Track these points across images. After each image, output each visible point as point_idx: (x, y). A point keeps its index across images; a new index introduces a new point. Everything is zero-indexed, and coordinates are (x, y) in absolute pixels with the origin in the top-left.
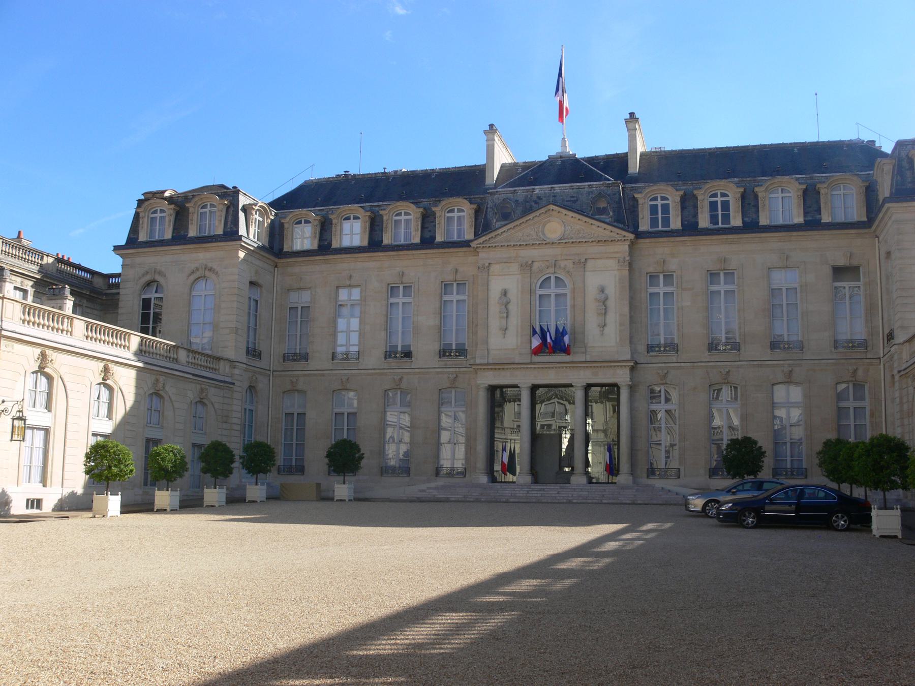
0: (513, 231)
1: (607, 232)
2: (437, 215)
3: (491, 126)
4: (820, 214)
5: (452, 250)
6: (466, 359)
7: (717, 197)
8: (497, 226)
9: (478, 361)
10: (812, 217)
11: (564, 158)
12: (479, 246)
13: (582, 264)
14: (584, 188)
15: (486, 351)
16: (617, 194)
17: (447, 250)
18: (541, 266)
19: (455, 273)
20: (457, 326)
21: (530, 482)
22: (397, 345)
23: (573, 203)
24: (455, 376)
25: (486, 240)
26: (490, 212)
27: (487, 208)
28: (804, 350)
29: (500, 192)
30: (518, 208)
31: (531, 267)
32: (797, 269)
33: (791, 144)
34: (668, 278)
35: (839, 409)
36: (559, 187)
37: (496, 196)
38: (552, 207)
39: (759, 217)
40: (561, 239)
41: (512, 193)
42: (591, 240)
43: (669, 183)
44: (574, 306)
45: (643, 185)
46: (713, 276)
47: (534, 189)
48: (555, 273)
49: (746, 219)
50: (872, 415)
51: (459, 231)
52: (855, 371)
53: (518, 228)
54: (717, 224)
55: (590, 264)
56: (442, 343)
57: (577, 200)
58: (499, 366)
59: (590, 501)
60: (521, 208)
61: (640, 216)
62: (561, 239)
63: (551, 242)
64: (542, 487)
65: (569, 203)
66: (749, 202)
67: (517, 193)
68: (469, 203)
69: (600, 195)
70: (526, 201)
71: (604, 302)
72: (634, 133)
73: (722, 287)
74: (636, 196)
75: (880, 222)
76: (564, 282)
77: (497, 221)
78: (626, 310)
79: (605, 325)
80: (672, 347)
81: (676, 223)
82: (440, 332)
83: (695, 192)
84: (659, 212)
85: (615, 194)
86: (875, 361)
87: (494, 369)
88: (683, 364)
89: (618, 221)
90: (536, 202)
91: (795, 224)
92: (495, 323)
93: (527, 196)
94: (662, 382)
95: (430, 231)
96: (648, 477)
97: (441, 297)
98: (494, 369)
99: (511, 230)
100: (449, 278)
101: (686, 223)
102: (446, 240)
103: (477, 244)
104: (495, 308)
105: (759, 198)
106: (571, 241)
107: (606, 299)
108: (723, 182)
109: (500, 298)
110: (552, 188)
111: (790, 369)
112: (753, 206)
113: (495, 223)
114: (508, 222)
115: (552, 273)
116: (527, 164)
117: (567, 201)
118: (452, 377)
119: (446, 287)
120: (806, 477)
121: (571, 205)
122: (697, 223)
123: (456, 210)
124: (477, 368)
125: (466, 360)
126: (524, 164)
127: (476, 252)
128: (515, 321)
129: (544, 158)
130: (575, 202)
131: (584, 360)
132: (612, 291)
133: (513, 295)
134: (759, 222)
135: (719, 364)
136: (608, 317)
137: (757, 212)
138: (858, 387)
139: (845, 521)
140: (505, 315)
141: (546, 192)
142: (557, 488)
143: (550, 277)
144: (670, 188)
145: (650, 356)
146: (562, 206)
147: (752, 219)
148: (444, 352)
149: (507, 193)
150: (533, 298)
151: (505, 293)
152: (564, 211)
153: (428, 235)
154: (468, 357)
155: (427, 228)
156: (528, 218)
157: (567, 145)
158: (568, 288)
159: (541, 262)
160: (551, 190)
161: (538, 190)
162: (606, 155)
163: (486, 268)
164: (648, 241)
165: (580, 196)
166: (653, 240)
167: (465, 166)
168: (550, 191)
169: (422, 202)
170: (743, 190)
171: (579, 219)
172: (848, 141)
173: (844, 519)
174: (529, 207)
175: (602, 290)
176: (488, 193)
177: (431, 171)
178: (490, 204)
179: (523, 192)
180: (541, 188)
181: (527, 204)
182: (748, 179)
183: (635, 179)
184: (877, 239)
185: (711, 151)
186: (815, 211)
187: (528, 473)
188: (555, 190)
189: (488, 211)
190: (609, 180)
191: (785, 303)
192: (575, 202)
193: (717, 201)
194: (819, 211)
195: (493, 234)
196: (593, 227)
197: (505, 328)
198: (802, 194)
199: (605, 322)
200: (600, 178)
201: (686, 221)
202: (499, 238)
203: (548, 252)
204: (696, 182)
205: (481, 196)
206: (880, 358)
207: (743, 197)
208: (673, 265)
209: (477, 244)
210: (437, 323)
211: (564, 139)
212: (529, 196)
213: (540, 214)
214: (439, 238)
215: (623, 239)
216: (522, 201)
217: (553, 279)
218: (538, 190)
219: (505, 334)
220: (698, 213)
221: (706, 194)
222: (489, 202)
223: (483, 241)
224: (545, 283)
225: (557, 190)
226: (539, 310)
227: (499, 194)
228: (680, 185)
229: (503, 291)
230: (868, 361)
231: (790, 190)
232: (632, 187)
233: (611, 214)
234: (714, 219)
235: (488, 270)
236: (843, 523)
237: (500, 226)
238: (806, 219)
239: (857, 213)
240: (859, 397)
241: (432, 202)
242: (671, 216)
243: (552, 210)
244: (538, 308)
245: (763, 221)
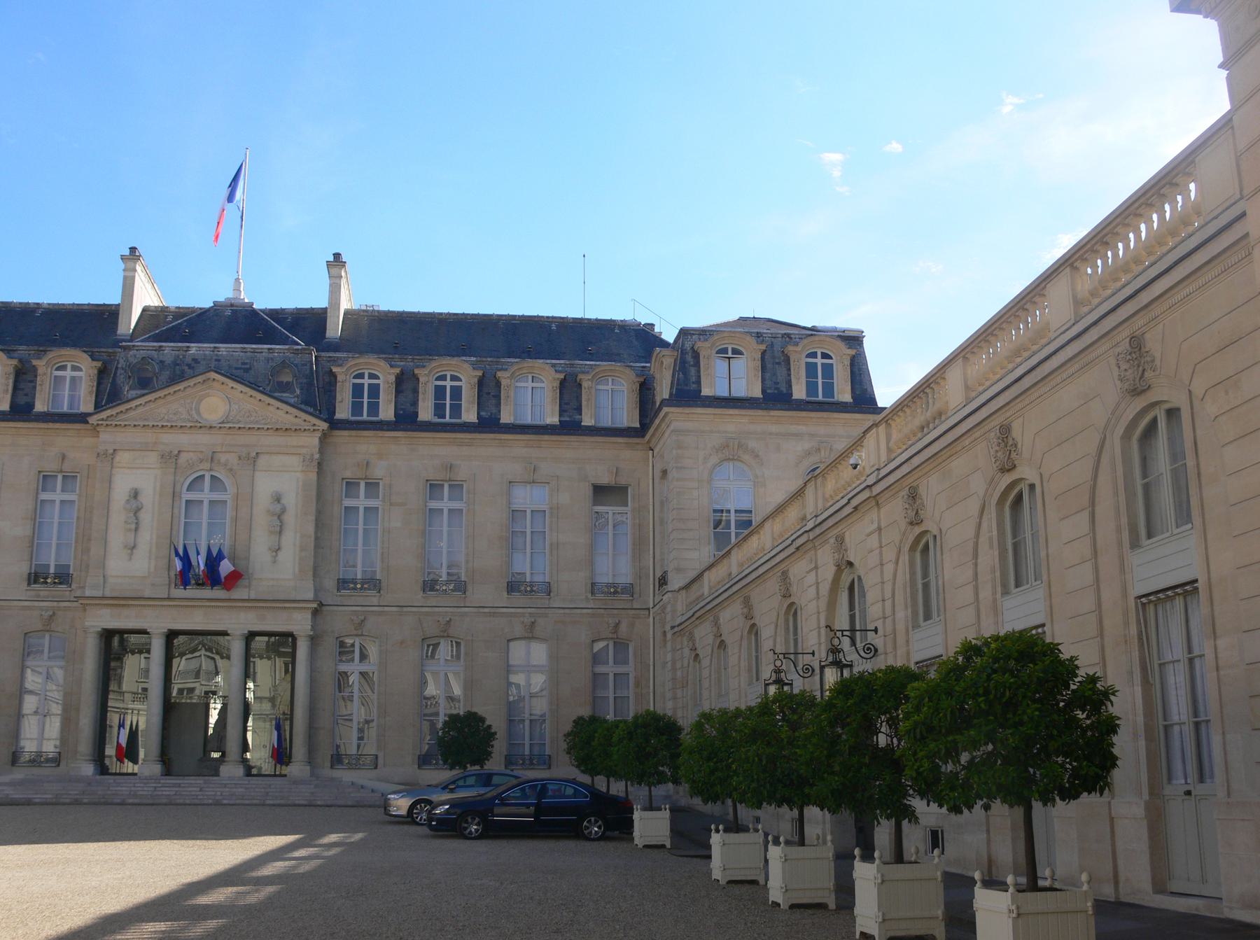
0: (153, 405)
2: (40, 371)
3: (133, 250)
4: (581, 414)
5: (58, 425)
6: (69, 589)
7: (446, 380)
8: (130, 396)
9: (88, 593)
10: (570, 417)
11: (237, 306)
12: (100, 422)
13: (252, 460)
14: (262, 352)
15: (102, 578)
17: (51, 425)
18: (191, 459)
19: (61, 459)
20: (59, 538)
21: (160, 774)
22: (49, 565)
24: (51, 613)
25: (112, 415)
26: (121, 374)
27: (117, 368)
28: (552, 594)
29: (138, 346)
30: (163, 372)
31: (176, 459)
32: (546, 485)
33: (548, 317)
34: (372, 487)
35: (595, 674)
36: (226, 348)
37: (131, 353)
38: (213, 375)
39: (500, 411)
40: (223, 423)
41: (155, 350)
42: (266, 427)
43: (381, 356)
44: (235, 520)
45: (345, 355)
46: (434, 488)
47: (188, 347)
48: (211, 470)
49: (483, 413)
50: (637, 684)
51: (72, 398)
52: (617, 625)
53: (161, 402)
54: (444, 417)
55: (262, 461)
56: (34, 563)
57: (250, 369)
58: (120, 601)
59: (247, 802)
60: (168, 373)
61: (339, 398)
62: (223, 423)
63: (208, 426)
64: (178, 782)
65: (239, 373)
66: (489, 390)
68: (90, 359)
69: (284, 364)
70: (175, 364)
71: (280, 516)
72: (337, 281)
73: (445, 504)
74: (334, 370)
75: (656, 430)
76: (224, 484)
77: (131, 388)
78: (311, 529)
79: (279, 549)
80: (372, 584)
81: (387, 412)
82: (32, 546)
83: (416, 371)
84: (365, 394)
85: (303, 365)
86: (642, 612)
87: (113, 605)
88: (386, 609)
89: (306, 403)
90: (190, 366)
91: (548, 425)
92: (117, 538)
93: (178, 356)
94: (355, 632)
95: (26, 395)
96: (332, 767)
97: (37, 494)
98: (113, 605)
99: (151, 403)
100: (51, 466)
101: (401, 412)
102: (50, 410)
103: (98, 420)
104: (118, 517)
105: (502, 386)
106: (237, 426)
107: (284, 510)
108: (455, 361)
109: (128, 501)
110: (215, 347)
111: (533, 620)
112: (493, 396)
113: (128, 391)
114: (146, 391)
115: (207, 470)
116: (182, 311)
117: (236, 369)
118: (47, 614)
119: (46, 480)
120: (549, 768)
121: (240, 374)
122: (416, 414)
123: (69, 367)
124: (85, 603)
125: (70, 591)
126: (177, 310)
127: (95, 430)
128: (147, 537)
129: (207, 304)
130: (247, 370)
131: (247, 598)
132: (291, 500)
133: (147, 498)
134: (500, 419)
135: (437, 609)
136: (284, 538)
137: (498, 405)
138: (621, 646)
139: (599, 827)
140: (133, 526)
141: (207, 352)
142: (198, 782)
143: (204, 475)
144: (382, 363)
145: (341, 596)
146: (228, 374)
147: (491, 414)
148: (36, 577)
149: (148, 350)
150: (176, 504)
151: (135, 494)
152: (231, 383)
153: (22, 400)
154: (74, 586)
155: (23, 389)
156: (178, 388)
157: (242, 289)
158: (228, 493)
159: (191, 454)
160: (213, 351)
161: (194, 348)
162: (297, 309)
163: (109, 456)
164: (347, 434)
165: (255, 364)
166: (353, 433)
167: (89, 304)
168: (212, 353)
169: (16, 350)
170: (563, 377)
171: (251, 396)
172: (621, 321)
173: (598, 824)
174: (179, 373)
175: (278, 499)
176: (120, 347)
177: (35, 306)
178: (122, 363)
180: (199, 347)
181: (178, 367)
182: (489, 359)
183: (335, 346)
184: (651, 452)
185: (441, 317)
186: (575, 409)
187: (155, 761)
188: (219, 351)
190: (299, 344)
191: (528, 531)
192: (247, 370)
193: (445, 386)
194: (579, 410)
195: (123, 408)
196: (271, 408)
197: (132, 545)
198: (559, 385)
199: (279, 545)
200: (284, 340)
201: (402, 409)
202: (132, 414)
203: (203, 439)
204: (418, 357)
205: (110, 350)
206: (649, 609)
207: (481, 383)
208: (379, 470)
209: (98, 420)
210: (28, 532)
211: (237, 280)
213: (195, 384)
214: (40, 407)
215: (312, 428)
216: (169, 362)
217: (207, 479)
218: (194, 349)
219: (131, 554)
220: (418, 400)
221: (433, 373)
222: (121, 361)
223: (108, 417)
224: (196, 483)
225: (223, 351)
226: (185, 522)
227: (137, 350)
228: (396, 360)
229: (133, 491)
230: (633, 612)
231: (544, 380)
232: (329, 357)
233: (298, 392)
234: (439, 410)
235: (112, 459)
236: (596, 829)
237: (134, 396)
238: (563, 419)
239: (627, 416)
240: (621, 659)
241: (33, 352)
242: (381, 400)
243: (214, 379)
244: (183, 520)
245: (506, 417)
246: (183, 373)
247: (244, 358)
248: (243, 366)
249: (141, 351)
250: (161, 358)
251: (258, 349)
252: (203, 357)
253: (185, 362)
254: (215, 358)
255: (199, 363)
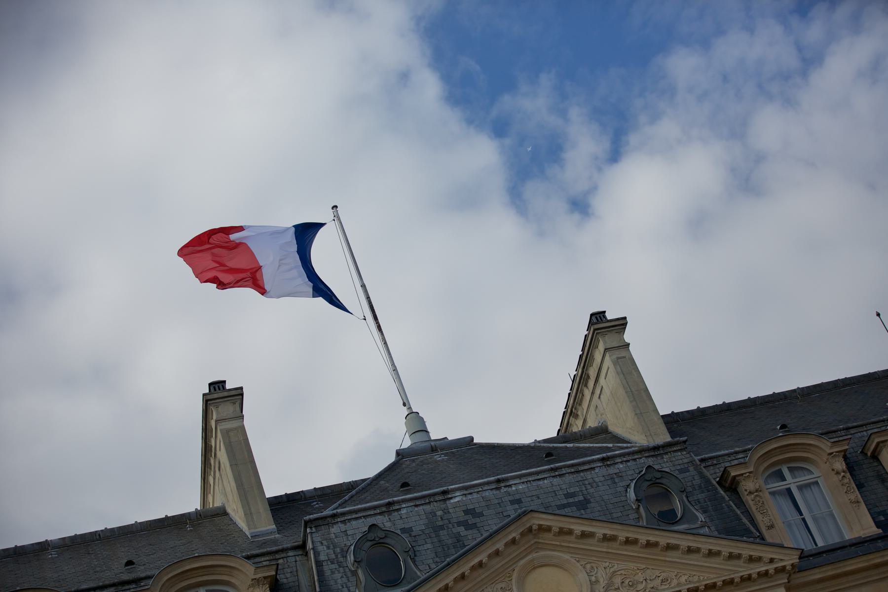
1: (714, 562)
14: (593, 469)
16: (691, 469)
23: (579, 510)
26: (333, 573)
37: (335, 529)
41: (381, 514)
60: (429, 546)
67: (399, 510)
85: (681, 471)
110: (498, 481)
179: (416, 506)
180: (466, 488)
188: (510, 486)
189: (328, 573)
212: (439, 513)
222: (320, 548)
233: (701, 517)
243: (541, 529)
246: (458, 541)
247: (564, 487)
248: (571, 500)
249: (354, 523)
250: (400, 524)
251: (584, 463)
252: (484, 504)
253: (455, 520)
254: (507, 499)
255: (481, 515)
